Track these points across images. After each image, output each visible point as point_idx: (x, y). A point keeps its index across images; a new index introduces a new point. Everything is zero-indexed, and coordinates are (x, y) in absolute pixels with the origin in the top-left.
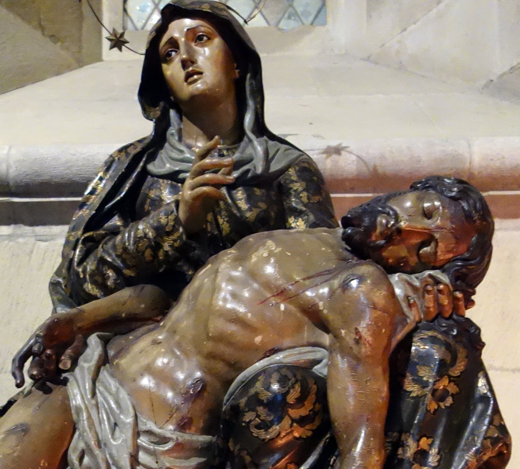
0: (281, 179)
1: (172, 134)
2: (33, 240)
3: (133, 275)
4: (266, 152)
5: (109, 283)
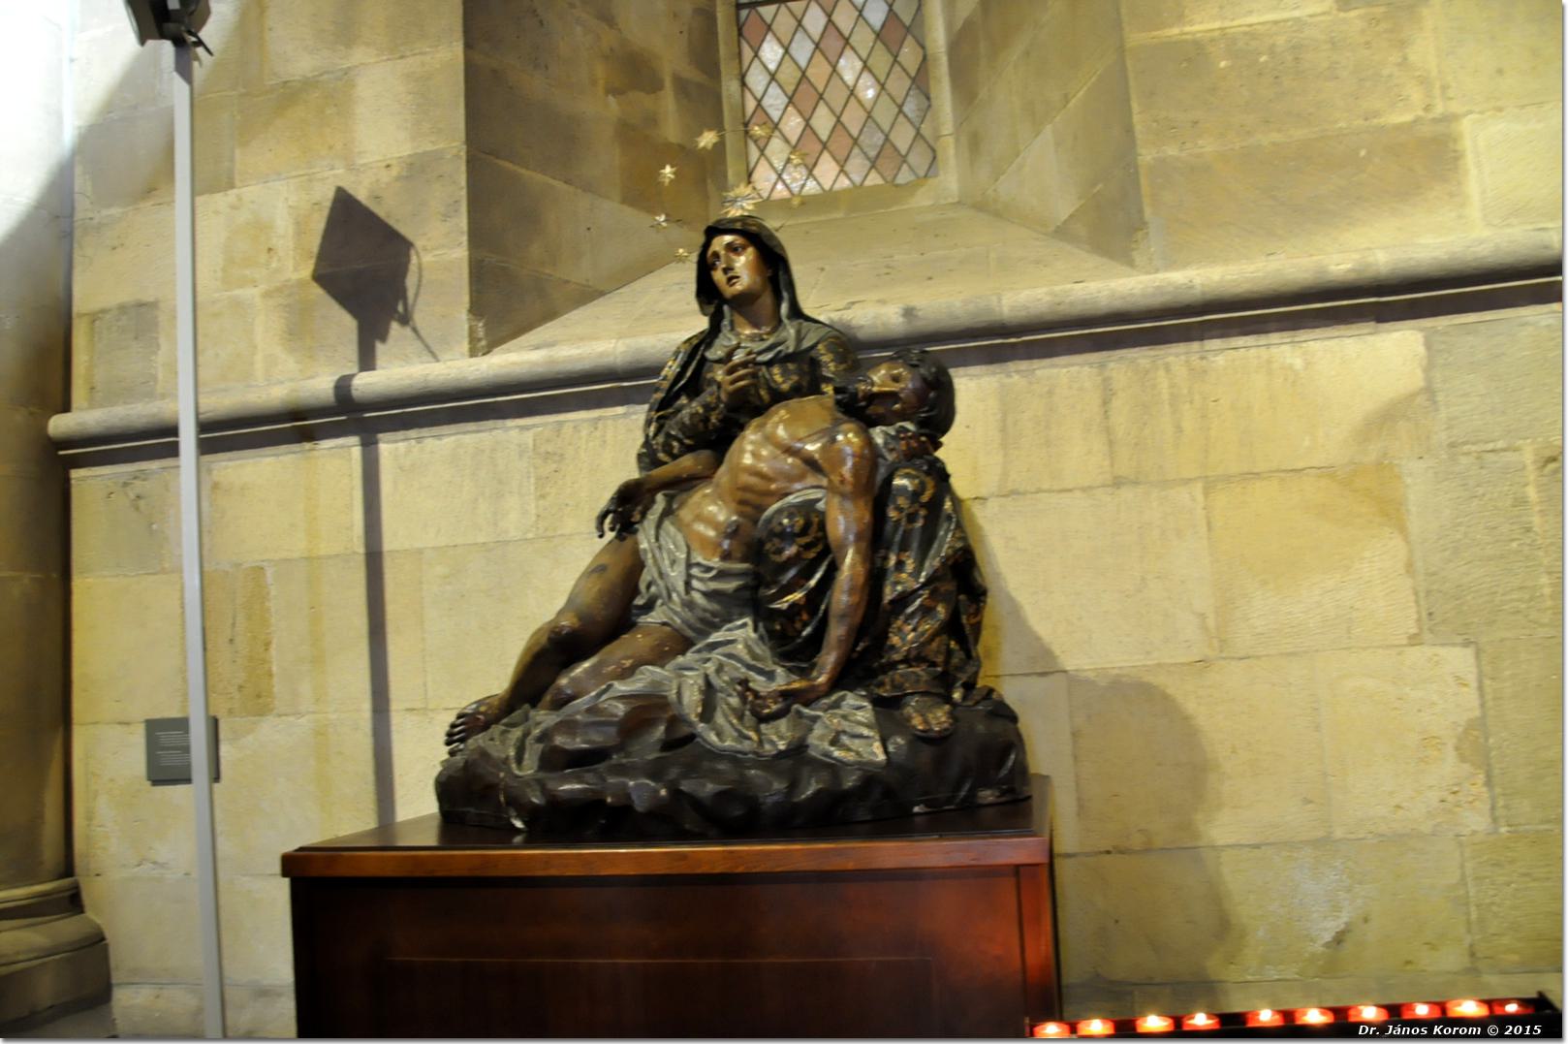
0: (813, 353)
1: (725, 326)
4: (798, 332)
5: (675, 451)
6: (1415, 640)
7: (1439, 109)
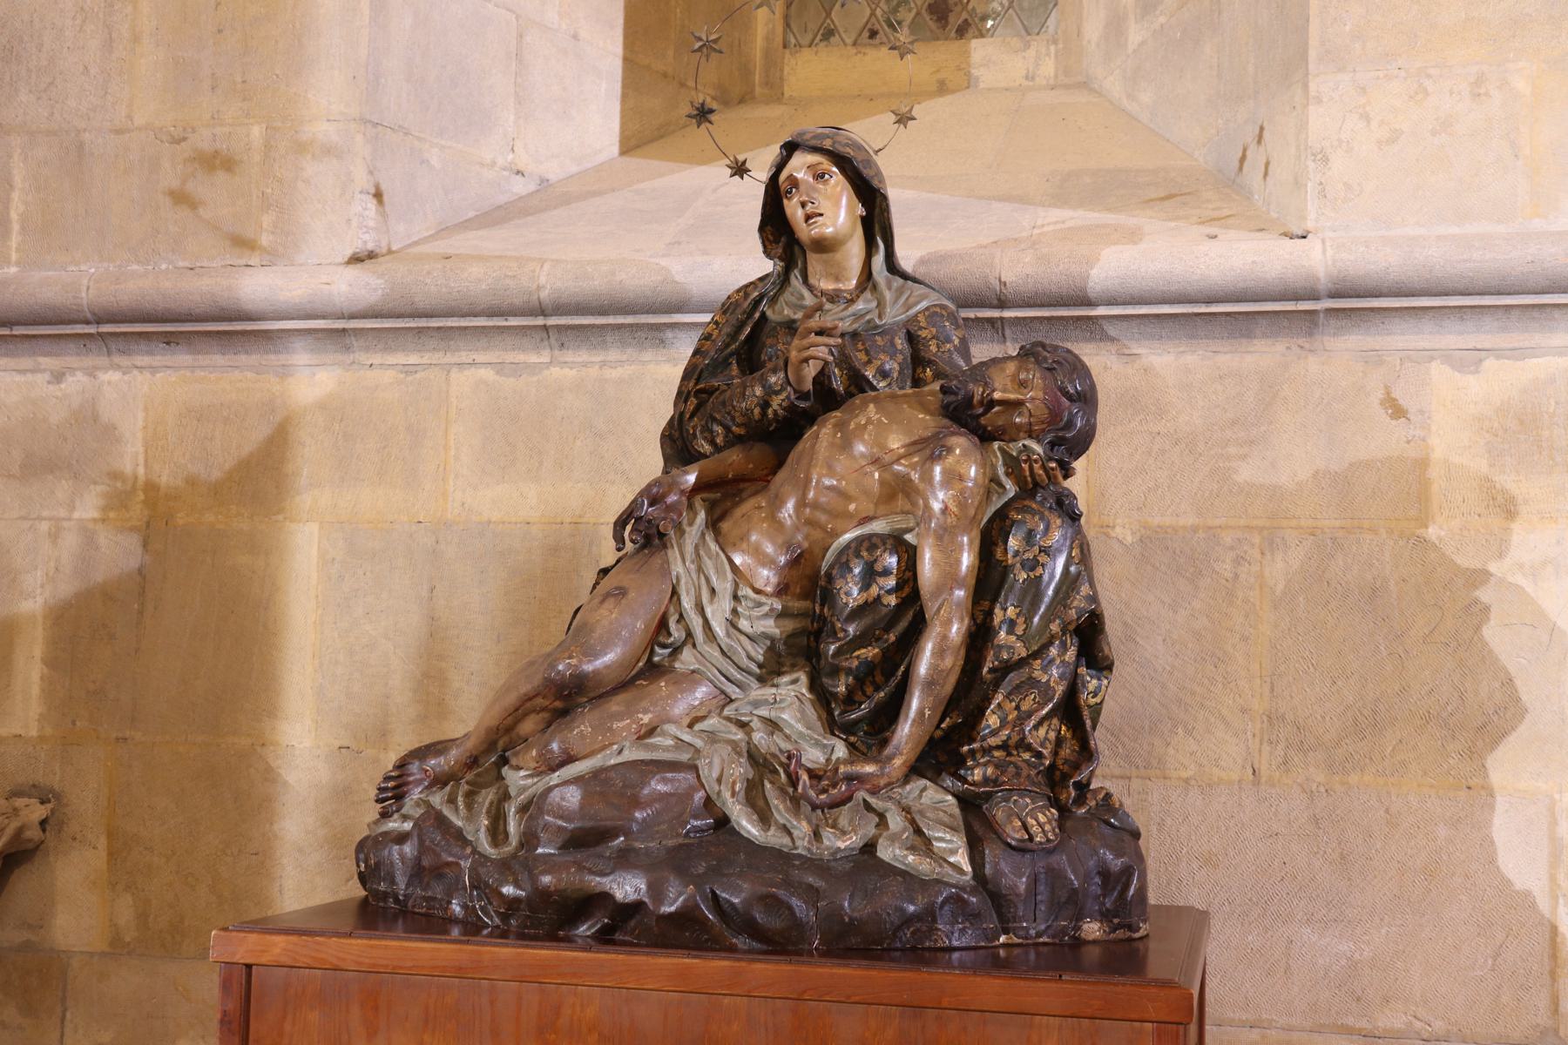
3: (742, 433)
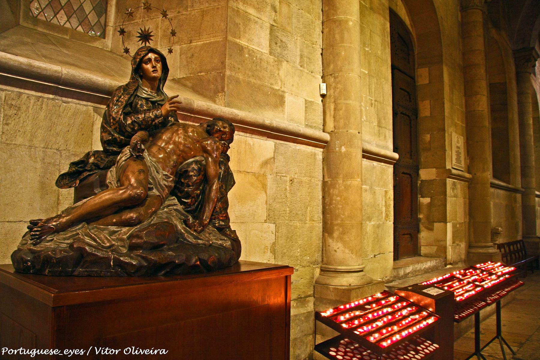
2: (61, 102)
6: (266, 221)
7: (283, 89)
